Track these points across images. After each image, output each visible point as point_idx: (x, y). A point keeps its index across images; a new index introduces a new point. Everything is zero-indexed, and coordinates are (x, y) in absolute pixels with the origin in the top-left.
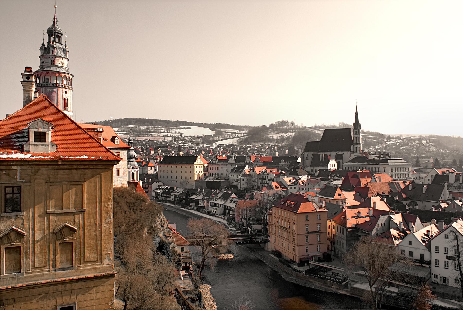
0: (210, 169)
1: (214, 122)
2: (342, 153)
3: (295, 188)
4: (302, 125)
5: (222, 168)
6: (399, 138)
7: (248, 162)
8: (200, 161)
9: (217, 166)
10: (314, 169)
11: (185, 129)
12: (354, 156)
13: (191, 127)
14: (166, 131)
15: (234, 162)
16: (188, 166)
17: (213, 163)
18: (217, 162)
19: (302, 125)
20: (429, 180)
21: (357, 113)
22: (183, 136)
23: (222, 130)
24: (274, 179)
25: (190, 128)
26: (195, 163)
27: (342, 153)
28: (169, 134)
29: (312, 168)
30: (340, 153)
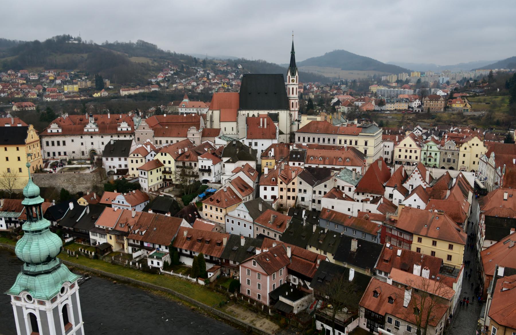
0: (47, 144)
2: (276, 112)
3: (273, 189)
4: (91, 41)
5: (73, 141)
9: (61, 139)
10: (253, 142)
12: (308, 119)
16: (12, 150)
17: (52, 135)
18: (60, 131)
19: (91, 41)
20: (400, 150)
24: (212, 168)
27: (276, 112)
29: (250, 141)
30: (273, 112)
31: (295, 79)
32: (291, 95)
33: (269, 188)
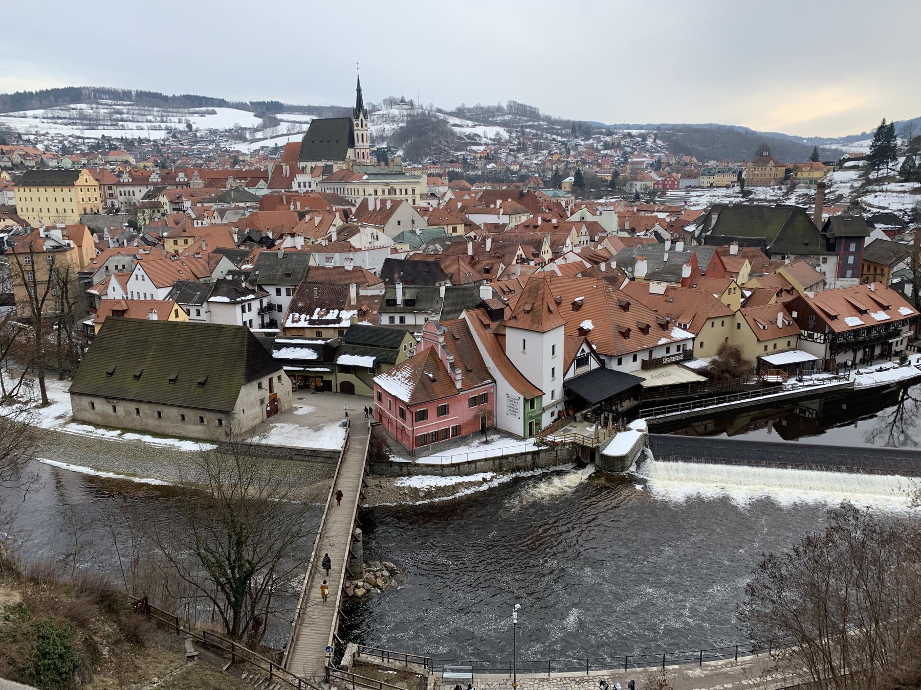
1: (267, 99)
4: (431, 105)
6: (609, 133)
7: (182, 180)
8: (85, 177)
9: (131, 189)
11: (202, 114)
13: (217, 109)
14: (159, 119)
15: (159, 180)
16: (66, 190)
18: (130, 180)
19: (431, 105)
21: (359, 91)
22: (194, 128)
23: (279, 116)
25: (214, 113)
26: (77, 183)
28: (163, 125)
30: (330, 163)
31: (359, 123)
32: (356, 144)
33: (200, 222)
